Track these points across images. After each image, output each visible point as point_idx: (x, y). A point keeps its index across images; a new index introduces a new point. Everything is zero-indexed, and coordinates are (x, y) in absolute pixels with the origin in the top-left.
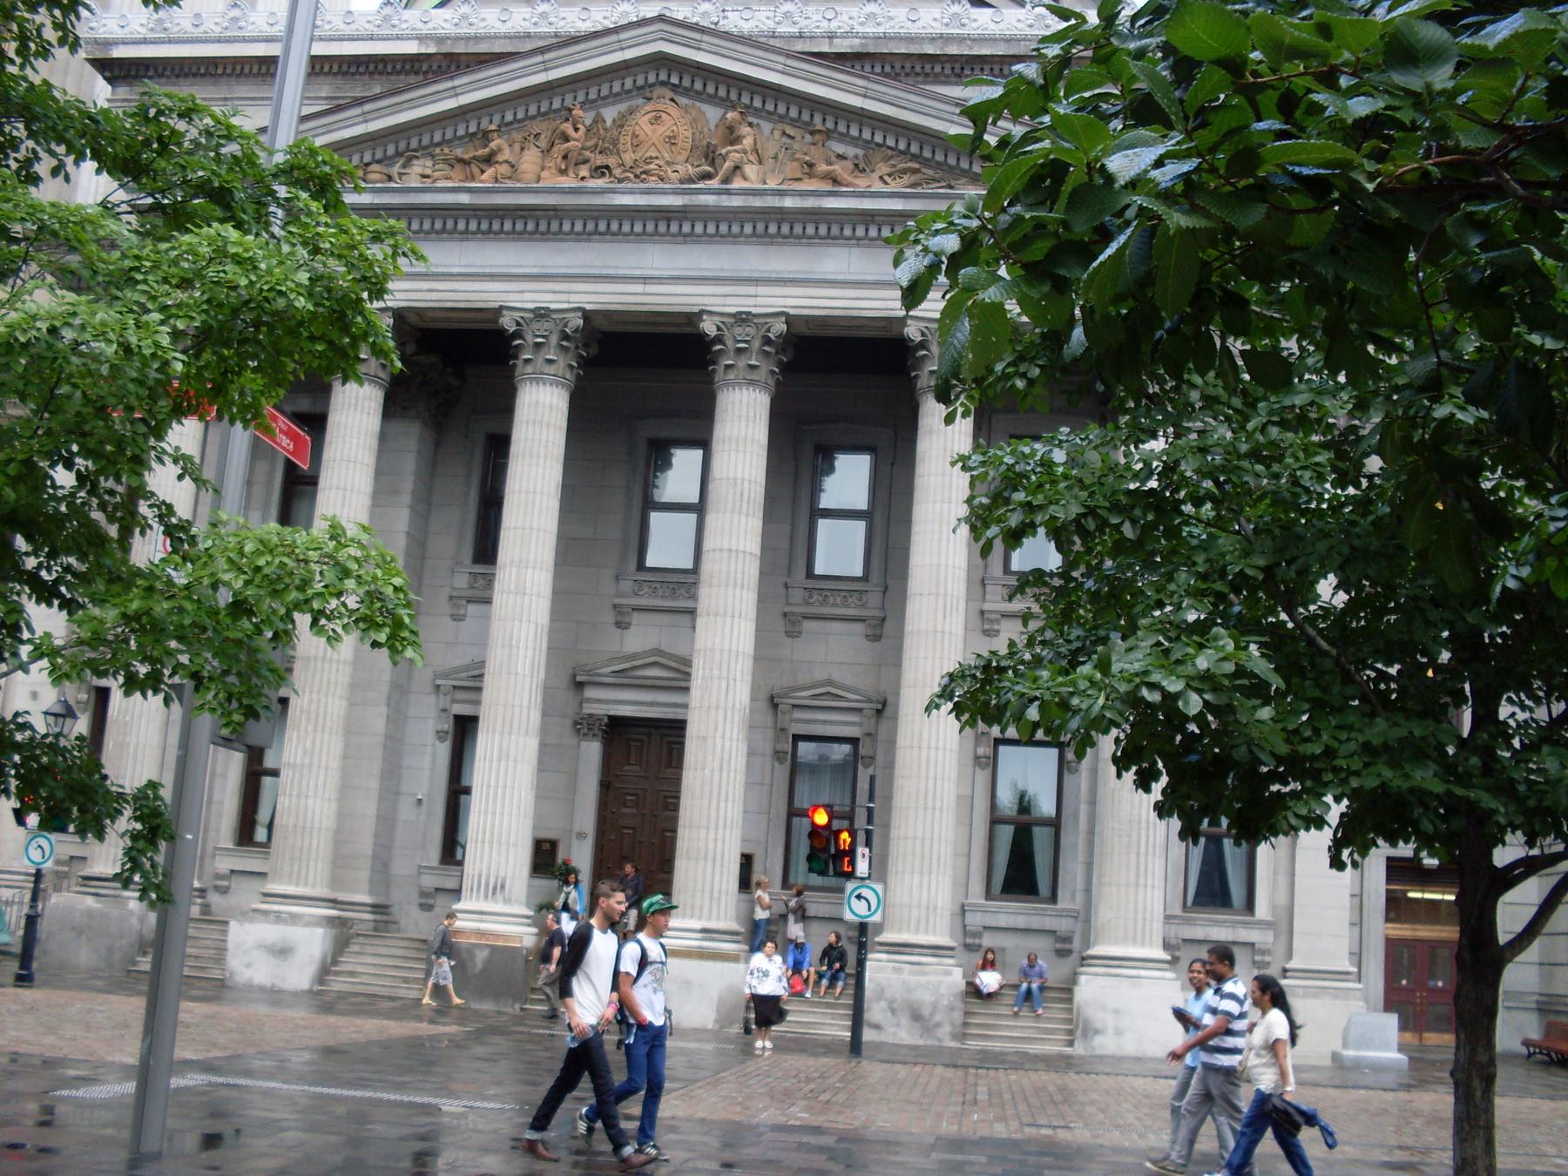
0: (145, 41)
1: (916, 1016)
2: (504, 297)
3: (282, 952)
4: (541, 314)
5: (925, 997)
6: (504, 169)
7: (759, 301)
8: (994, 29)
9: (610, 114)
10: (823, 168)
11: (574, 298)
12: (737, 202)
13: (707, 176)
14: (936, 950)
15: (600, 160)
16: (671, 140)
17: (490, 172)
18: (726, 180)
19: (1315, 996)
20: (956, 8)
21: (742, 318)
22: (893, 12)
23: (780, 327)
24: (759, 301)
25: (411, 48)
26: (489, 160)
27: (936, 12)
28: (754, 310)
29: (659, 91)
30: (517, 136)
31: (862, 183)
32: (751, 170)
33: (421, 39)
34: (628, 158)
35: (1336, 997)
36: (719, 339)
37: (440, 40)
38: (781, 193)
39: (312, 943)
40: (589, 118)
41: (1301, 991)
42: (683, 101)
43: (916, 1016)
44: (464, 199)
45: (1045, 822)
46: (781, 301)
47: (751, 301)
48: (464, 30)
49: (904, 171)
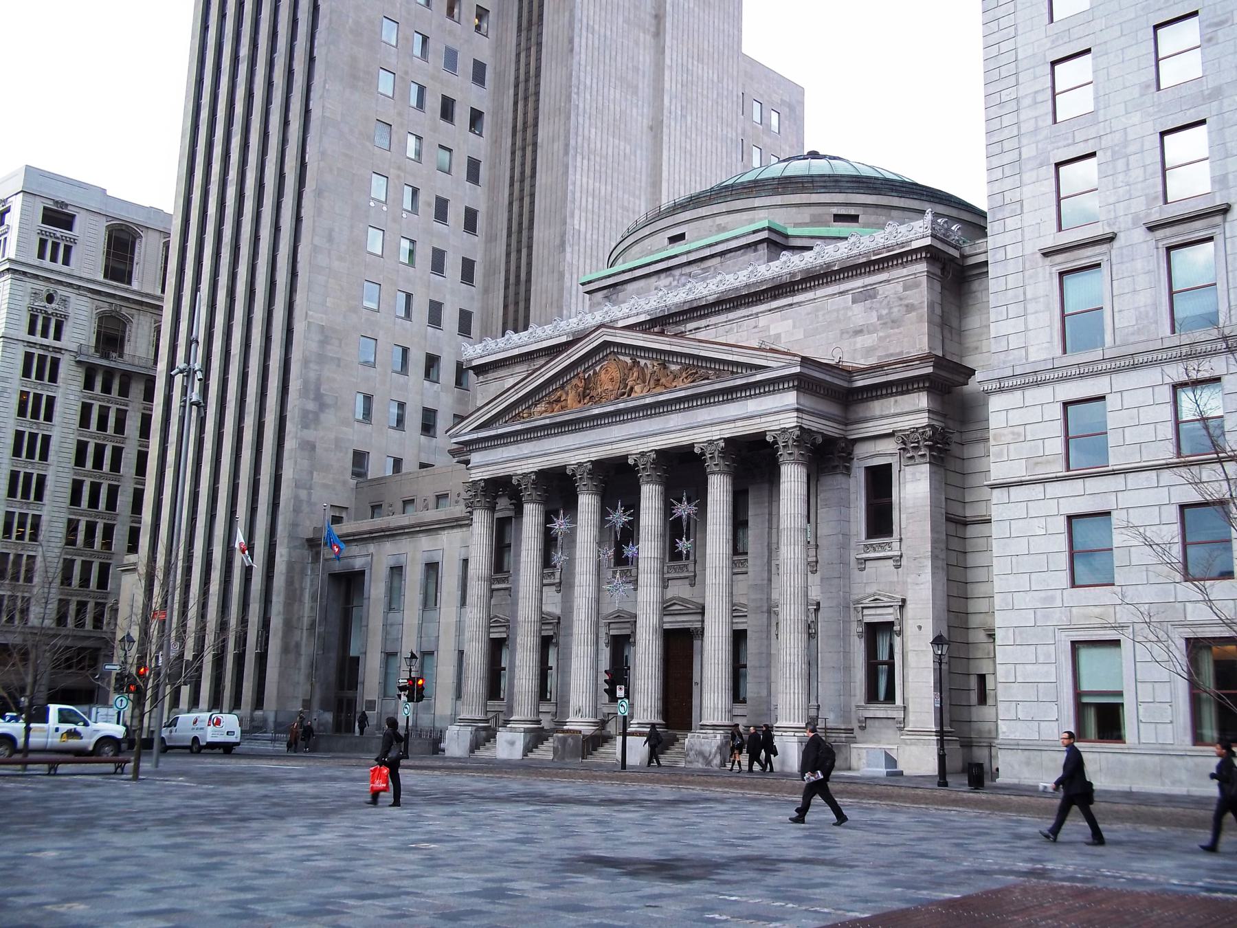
0: (481, 357)
1: (705, 758)
2: (568, 459)
3: (512, 743)
4: (580, 465)
5: (706, 749)
6: (563, 404)
7: (649, 445)
8: (768, 275)
9: (598, 369)
10: (663, 380)
11: (592, 455)
12: (630, 404)
13: (623, 394)
14: (714, 727)
15: (593, 393)
16: (612, 380)
17: (559, 405)
18: (629, 395)
19: (915, 744)
20: (750, 268)
21: (643, 454)
22: (727, 277)
23: (653, 455)
24: (649, 445)
25: (564, 339)
26: (558, 401)
27: (745, 272)
28: (645, 450)
29: (610, 357)
30: (569, 387)
31: (674, 384)
32: (637, 388)
33: (567, 334)
34: (599, 390)
35: (924, 744)
36: (636, 465)
37: (573, 334)
38: (644, 397)
39: (520, 740)
40: (591, 372)
41: (908, 742)
42: (621, 357)
43: (705, 758)
44: (547, 421)
45: (884, 663)
46: (655, 444)
47: (646, 446)
48: (581, 327)
49: (691, 374)
